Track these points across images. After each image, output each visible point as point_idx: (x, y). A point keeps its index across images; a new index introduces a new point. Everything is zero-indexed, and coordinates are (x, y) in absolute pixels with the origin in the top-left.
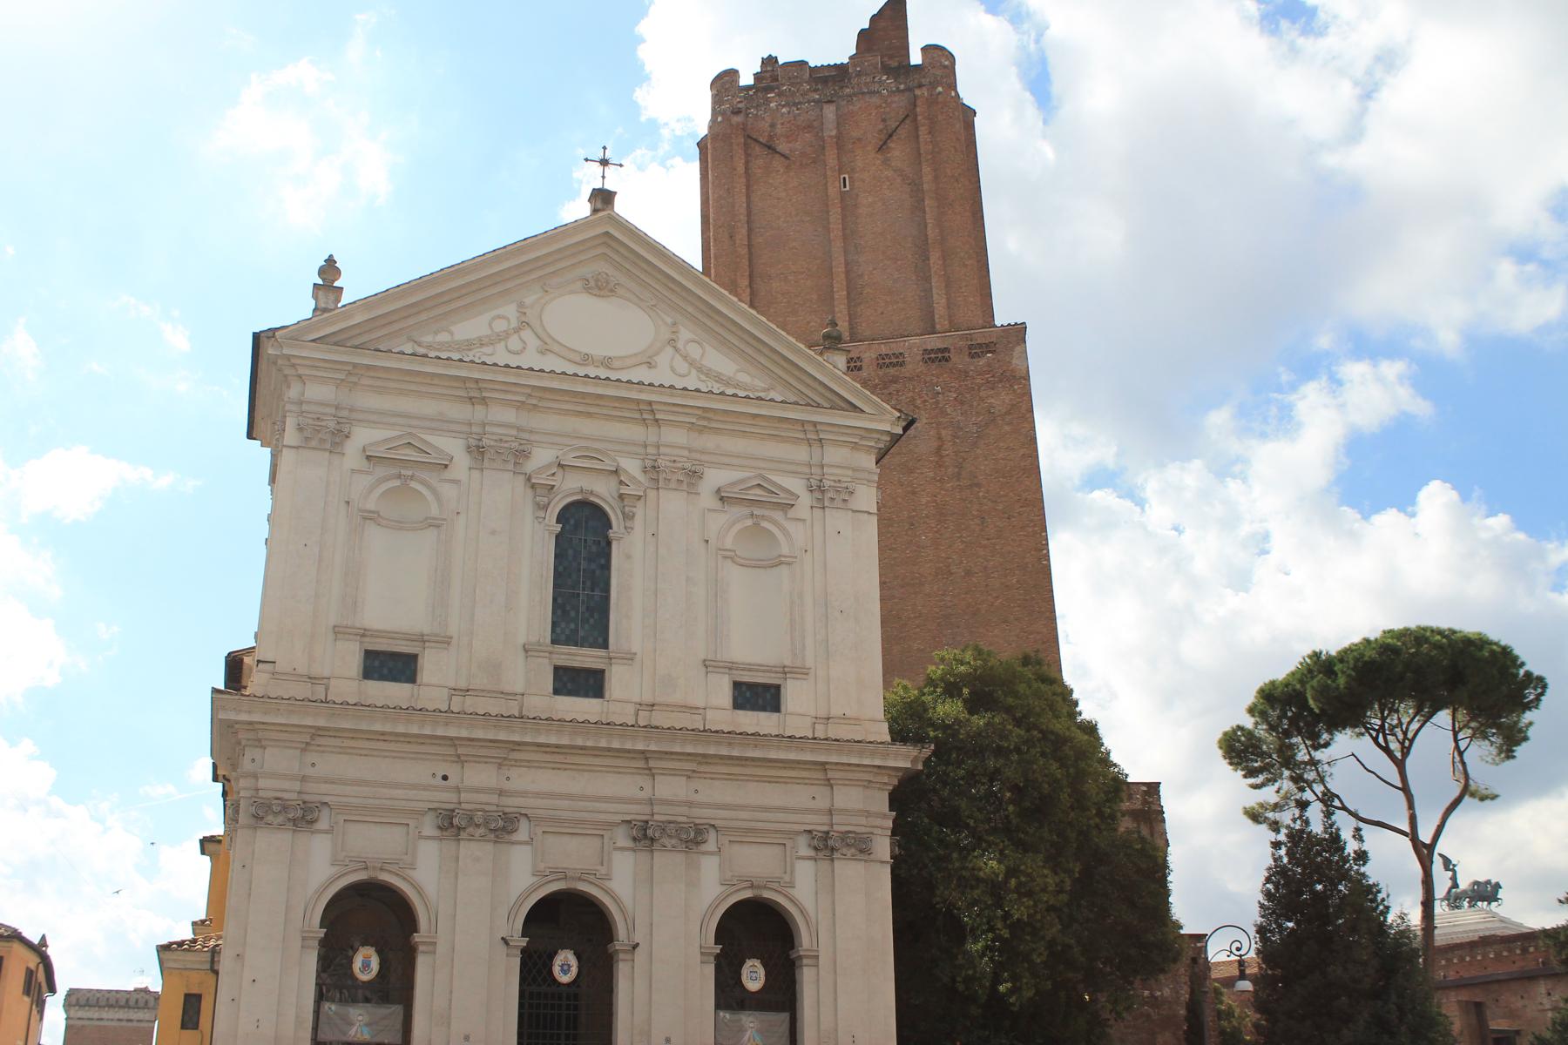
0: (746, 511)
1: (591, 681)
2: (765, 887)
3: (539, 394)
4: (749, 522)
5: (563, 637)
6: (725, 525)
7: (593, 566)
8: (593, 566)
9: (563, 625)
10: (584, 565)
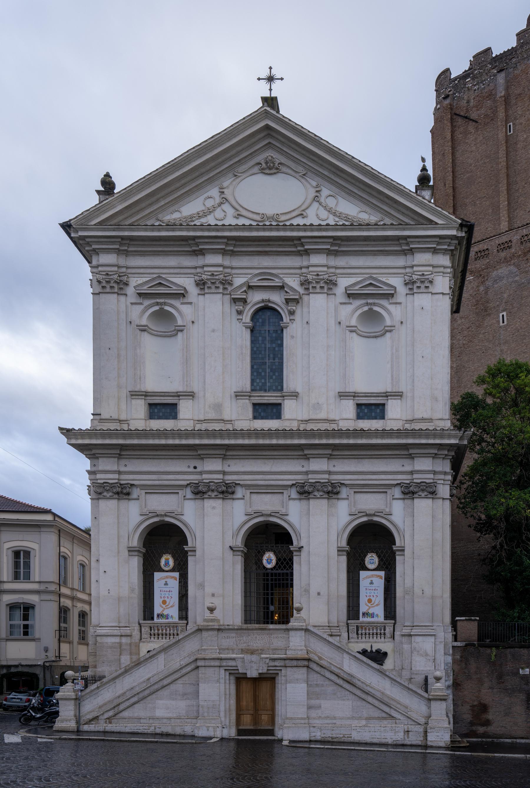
0: (363, 301)
1: (275, 410)
2: (374, 515)
3: (237, 244)
4: (366, 308)
5: (258, 388)
6: (350, 313)
7: (274, 345)
8: (274, 345)
9: (258, 381)
10: (268, 345)
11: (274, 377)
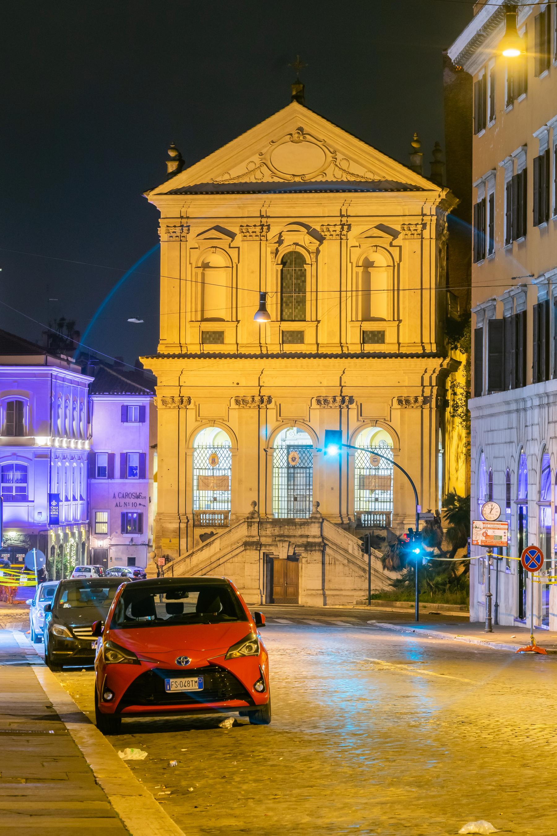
1: (299, 336)
8: (299, 281)
9: (286, 310)
11: (299, 307)
